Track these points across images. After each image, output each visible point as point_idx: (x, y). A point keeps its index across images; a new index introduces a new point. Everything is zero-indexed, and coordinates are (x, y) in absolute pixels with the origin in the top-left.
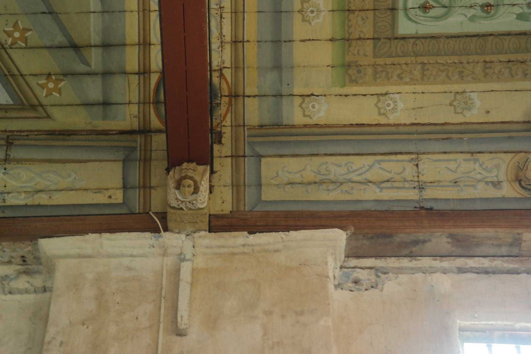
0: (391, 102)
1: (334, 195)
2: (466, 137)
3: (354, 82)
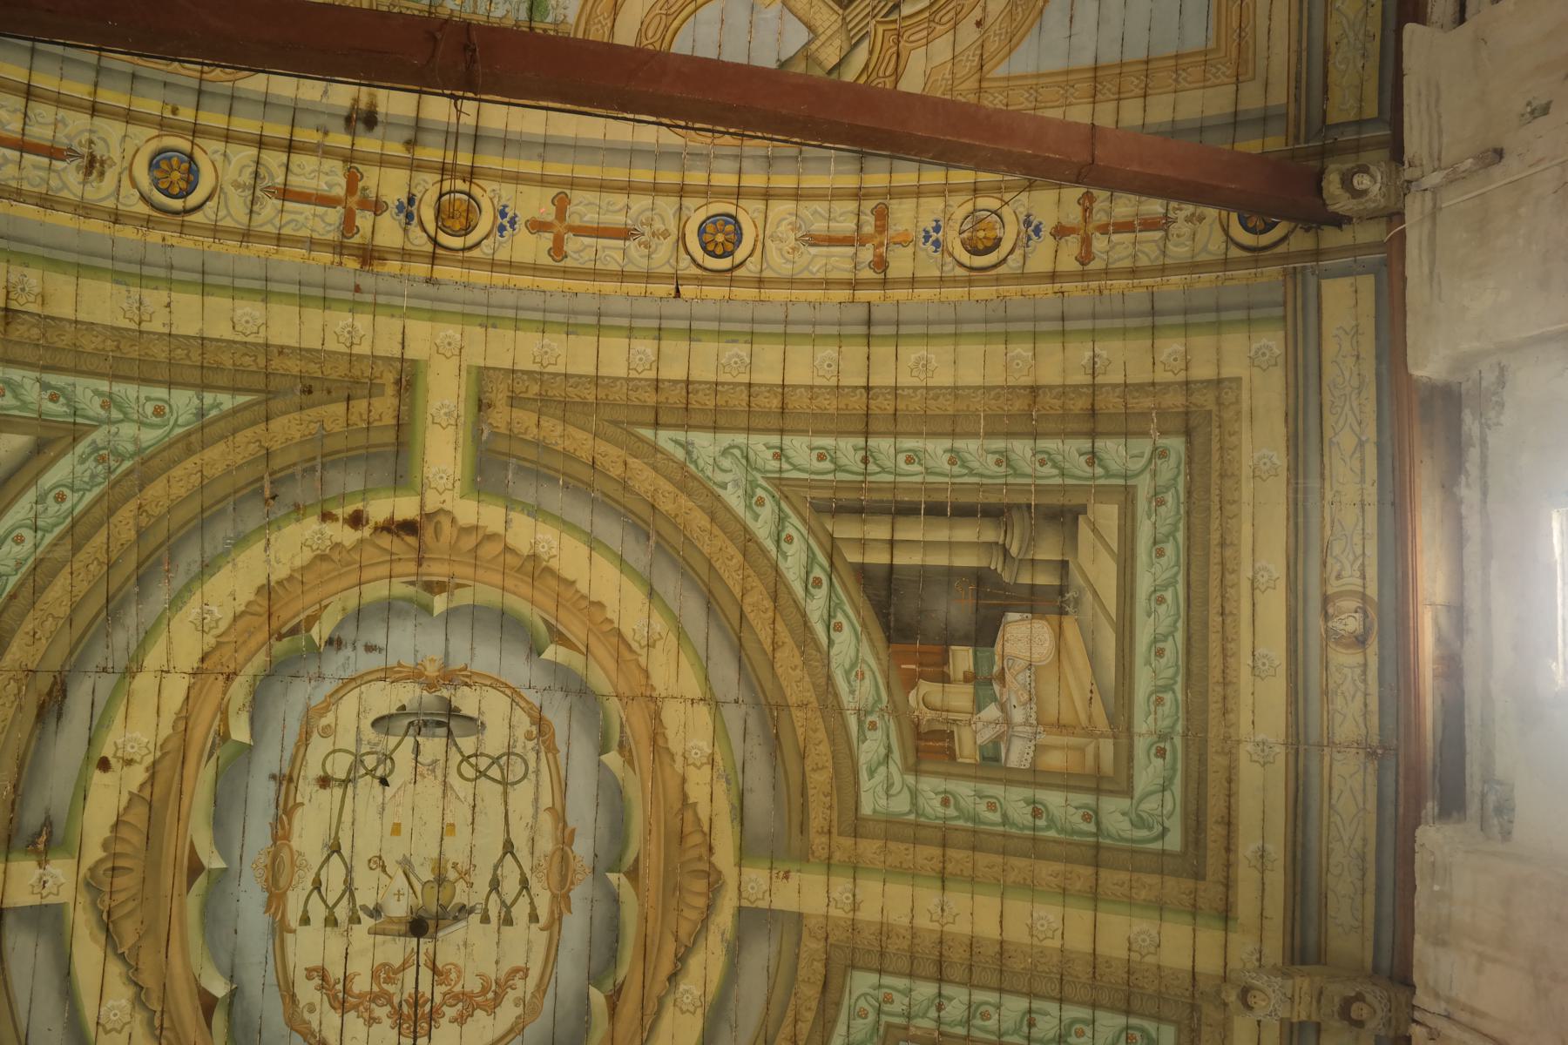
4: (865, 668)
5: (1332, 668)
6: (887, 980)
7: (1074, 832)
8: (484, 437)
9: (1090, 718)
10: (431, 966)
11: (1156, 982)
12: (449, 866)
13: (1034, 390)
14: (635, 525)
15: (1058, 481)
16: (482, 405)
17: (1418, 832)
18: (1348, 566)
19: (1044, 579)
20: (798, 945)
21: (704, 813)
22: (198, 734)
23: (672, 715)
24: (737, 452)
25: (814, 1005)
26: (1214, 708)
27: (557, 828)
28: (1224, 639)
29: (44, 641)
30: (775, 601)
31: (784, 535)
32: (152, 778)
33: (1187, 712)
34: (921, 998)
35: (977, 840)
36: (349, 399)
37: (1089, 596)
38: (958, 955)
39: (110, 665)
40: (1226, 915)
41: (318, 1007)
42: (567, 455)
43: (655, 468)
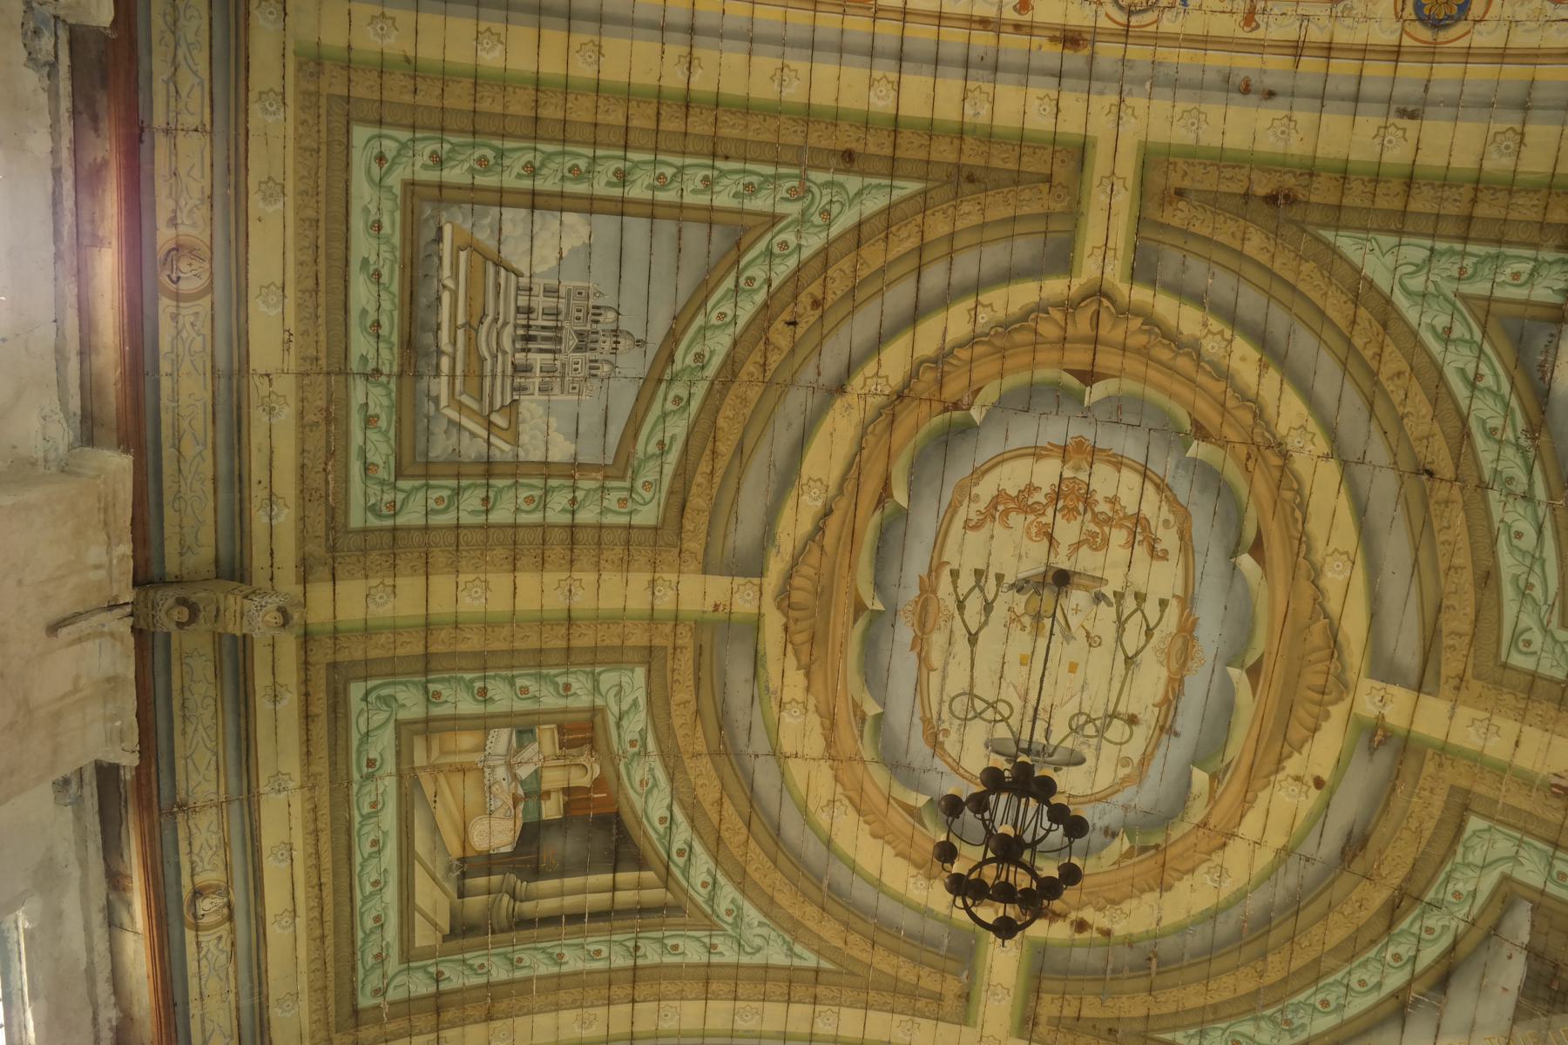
0: (274, 108)
1: (158, 23)
2: (231, 192)
3: (300, 67)
4: (639, 790)
5: (222, 866)
6: (624, 520)
7: (448, 680)
8: (966, 973)
9: (436, 781)
10: (1055, 543)
11: (368, 563)
12: (1028, 629)
13: (489, 1017)
14: (840, 896)
15: (467, 956)
16: (966, 997)
17: (136, 763)
18: (212, 948)
19: (481, 881)
20: (707, 544)
21: (791, 661)
22: (1236, 787)
23: (816, 744)
24: (748, 949)
25: (694, 489)
26: (325, 810)
27: (927, 652)
28: (318, 867)
29: (1354, 898)
30: (719, 837)
31: (710, 887)
32: (1280, 761)
33: (348, 802)
34: (591, 507)
35: (538, 659)
36: (1078, 1019)
37: (439, 876)
38: (556, 552)
39: (1302, 862)
40: (307, 638)
41: (1160, 523)
42: (897, 953)
43: (820, 937)
